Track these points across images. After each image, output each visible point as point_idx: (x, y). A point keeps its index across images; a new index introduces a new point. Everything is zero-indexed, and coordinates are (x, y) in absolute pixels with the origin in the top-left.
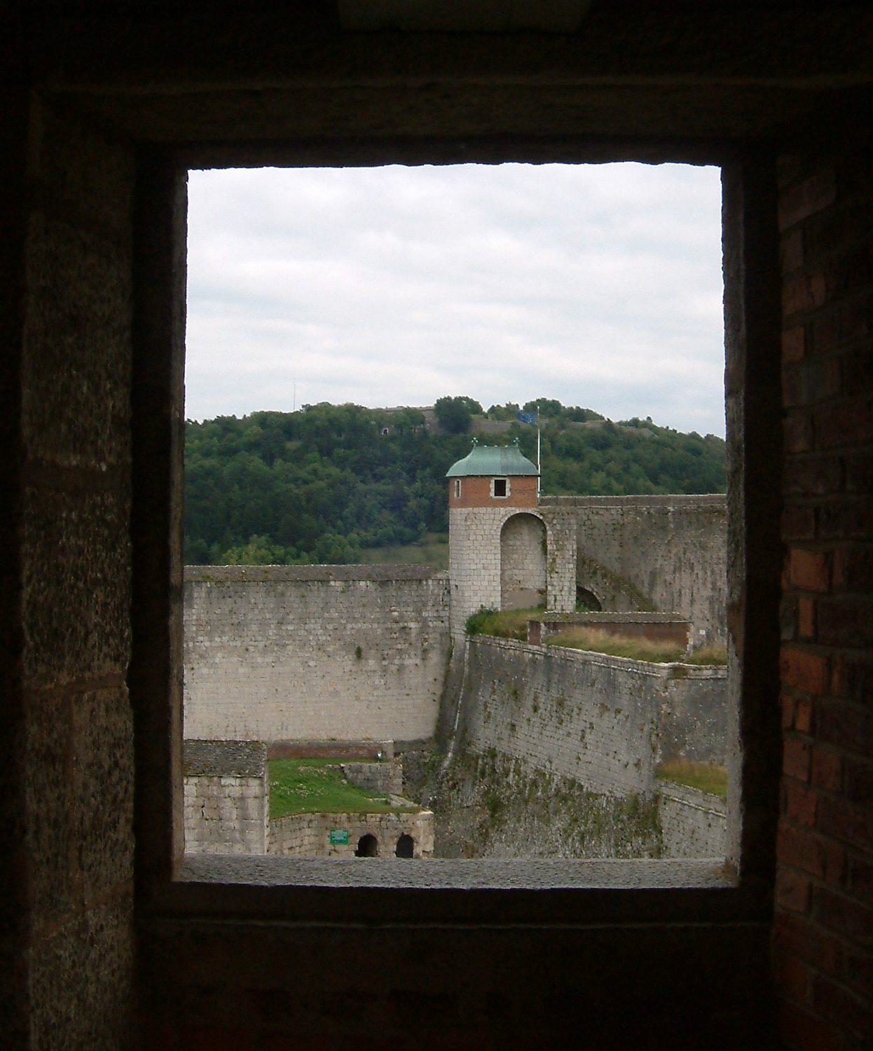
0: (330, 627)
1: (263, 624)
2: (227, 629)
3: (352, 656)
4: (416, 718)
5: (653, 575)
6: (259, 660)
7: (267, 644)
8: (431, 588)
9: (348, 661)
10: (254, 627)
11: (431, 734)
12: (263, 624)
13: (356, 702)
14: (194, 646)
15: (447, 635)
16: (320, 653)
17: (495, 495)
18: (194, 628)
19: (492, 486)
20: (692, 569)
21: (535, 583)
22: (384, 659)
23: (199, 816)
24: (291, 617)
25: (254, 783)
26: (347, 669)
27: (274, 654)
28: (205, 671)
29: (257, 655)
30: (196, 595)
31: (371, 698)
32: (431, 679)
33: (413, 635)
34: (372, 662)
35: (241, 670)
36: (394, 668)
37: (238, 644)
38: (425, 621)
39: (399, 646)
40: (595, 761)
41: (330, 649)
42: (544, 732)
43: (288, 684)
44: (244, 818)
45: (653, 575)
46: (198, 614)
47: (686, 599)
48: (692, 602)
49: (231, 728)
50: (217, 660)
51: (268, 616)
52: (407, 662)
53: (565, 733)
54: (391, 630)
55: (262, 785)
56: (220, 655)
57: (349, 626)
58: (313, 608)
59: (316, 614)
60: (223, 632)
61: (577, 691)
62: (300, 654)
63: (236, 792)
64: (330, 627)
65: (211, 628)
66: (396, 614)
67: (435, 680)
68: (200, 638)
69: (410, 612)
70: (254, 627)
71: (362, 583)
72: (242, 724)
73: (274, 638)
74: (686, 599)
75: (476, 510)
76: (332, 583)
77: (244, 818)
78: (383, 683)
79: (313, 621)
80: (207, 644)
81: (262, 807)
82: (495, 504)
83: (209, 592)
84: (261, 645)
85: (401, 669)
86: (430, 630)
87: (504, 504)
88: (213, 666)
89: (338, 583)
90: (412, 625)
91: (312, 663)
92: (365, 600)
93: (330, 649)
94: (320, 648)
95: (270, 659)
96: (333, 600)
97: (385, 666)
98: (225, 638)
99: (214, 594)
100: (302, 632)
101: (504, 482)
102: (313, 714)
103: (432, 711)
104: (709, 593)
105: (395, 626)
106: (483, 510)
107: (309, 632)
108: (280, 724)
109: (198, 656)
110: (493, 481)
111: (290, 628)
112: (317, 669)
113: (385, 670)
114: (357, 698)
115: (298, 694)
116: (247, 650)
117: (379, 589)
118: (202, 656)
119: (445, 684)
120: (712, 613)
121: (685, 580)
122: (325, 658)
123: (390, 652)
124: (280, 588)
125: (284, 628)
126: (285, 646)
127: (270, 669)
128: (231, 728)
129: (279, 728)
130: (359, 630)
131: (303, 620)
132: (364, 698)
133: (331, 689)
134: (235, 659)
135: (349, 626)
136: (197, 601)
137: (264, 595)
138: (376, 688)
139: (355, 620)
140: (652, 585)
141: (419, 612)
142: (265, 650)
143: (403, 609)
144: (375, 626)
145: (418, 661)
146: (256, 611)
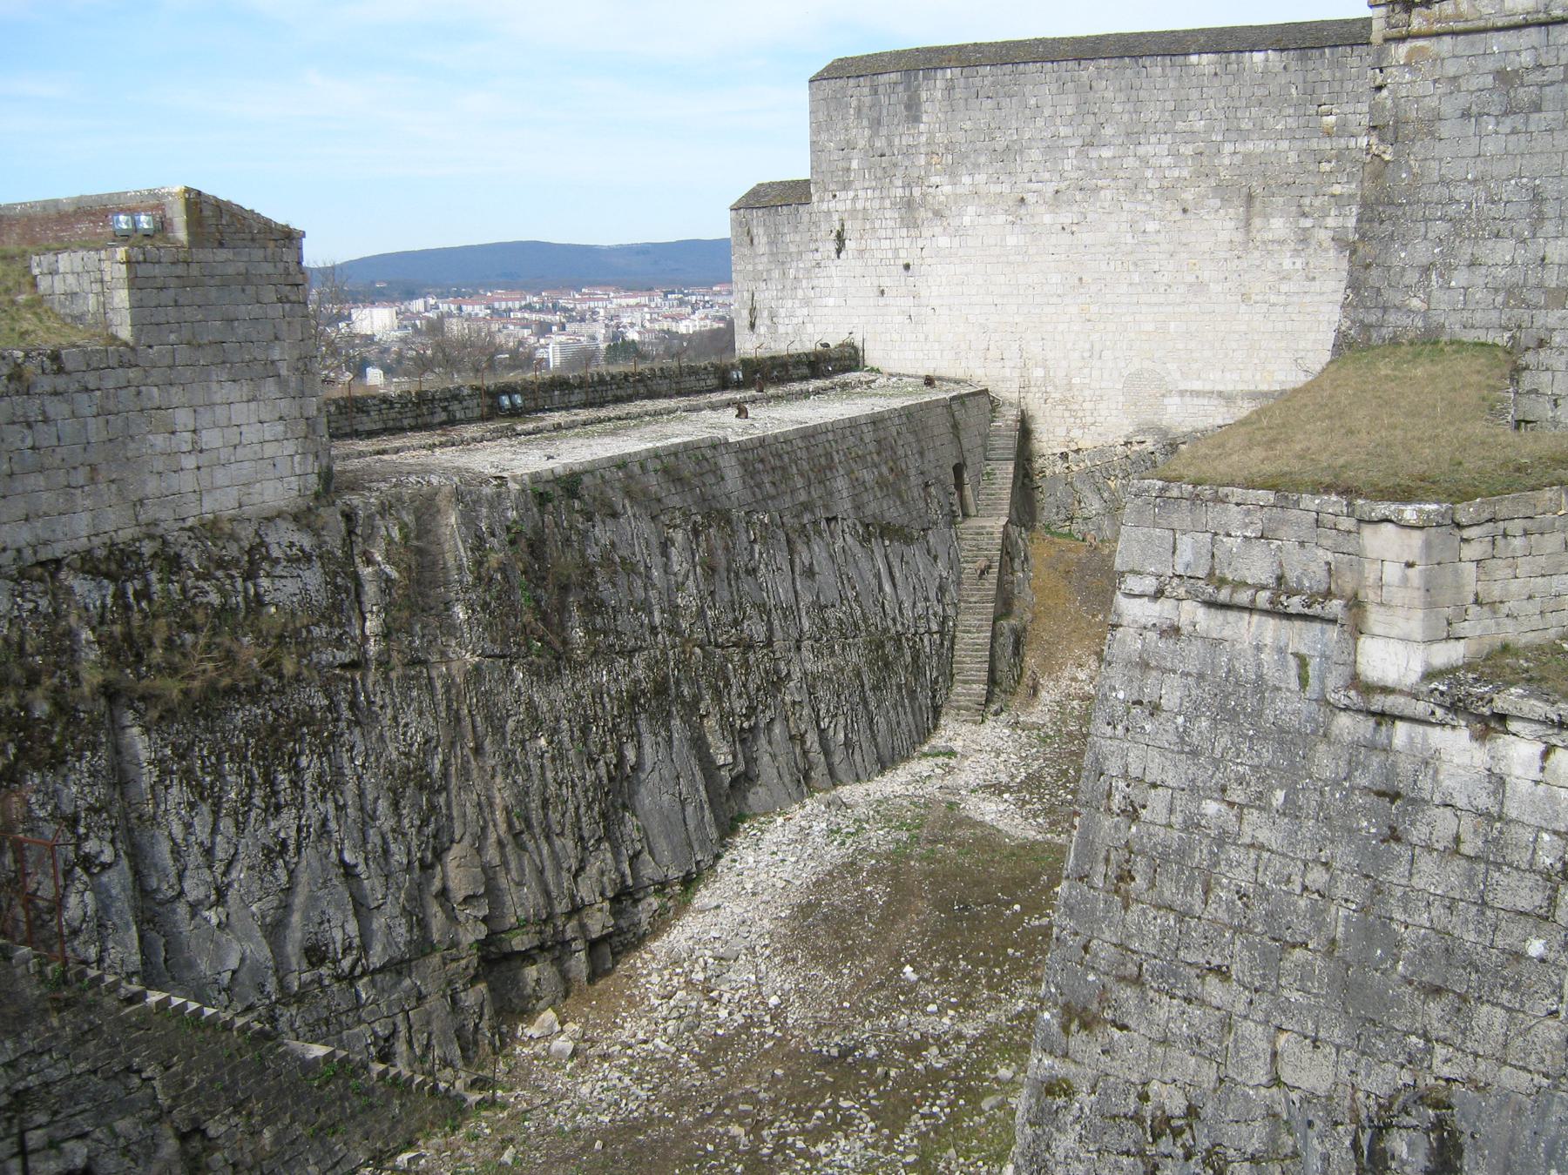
0: (1188, 150)
1: (1053, 148)
2: (982, 159)
6: (1047, 219)
7: (1063, 186)
9: (1222, 224)
10: (1035, 154)
12: (1053, 148)
13: (1243, 307)
14: (924, 195)
16: (1168, 206)
18: (922, 160)
22: (1305, 215)
24: (1108, 131)
26: (1224, 236)
27: (1075, 208)
28: (943, 241)
29: (1042, 209)
30: (924, 95)
31: (1273, 299)
35: (1011, 240)
37: (1006, 188)
39: (1337, 189)
41: (1188, 196)
43: (1104, 267)
46: (931, 134)
49: (994, 353)
50: (967, 220)
51: (1063, 131)
56: (971, 210)
57: (1228, 148)
58: (1151, 114)
59: (1160, 125)
60: (977, 166)
64: (1188, 150)
65: (957, 160)
66: (1331, 119)
68: (935, 180)
70: (1035, 154)
71: (1258, 57)
76: (1194, 59)
78: (1298, 266)
79: (1153, 139)
80: (947, 189)
83: (950, 88)
84: (1050, 189)
88: (960, 232)
89: (1205, 58)
92: (1260, 92)
93: (1188, 196)
94: (1168, 191)
95: (1066, 217)
96: (1195, 94)
97: (1305, 230)
98: (981, 178)
99: (958, 94)
100: (1130, 162)
102: (1150, 327)
105: (1326, 145)
107: (1144, 161)
108: (1088, 346)
109: (930, 215)
111: (1106, 153)
112: (1160, 238)
113: (1304, 238)
114: (1245, 297)
116: (1022, 200)
117: (1293, 66)
118: (938, 214)
122: (1178, 215)
123: (1317, 203)
125: (1093, 153)
126: (1097, 189)
127: (1065, 238)
128: (994, 353)
129: (1087, 354)
131: (1133, 136)
132: (1259, 298)
133: (1191, 279)
134: (1001, 219)
135: (1228, 148)
136: (927, 107)
137: (1054, 88)
139: (1244, 135)
143: (1348, 108)
144: (1284, 145)
146: (1040, 122)
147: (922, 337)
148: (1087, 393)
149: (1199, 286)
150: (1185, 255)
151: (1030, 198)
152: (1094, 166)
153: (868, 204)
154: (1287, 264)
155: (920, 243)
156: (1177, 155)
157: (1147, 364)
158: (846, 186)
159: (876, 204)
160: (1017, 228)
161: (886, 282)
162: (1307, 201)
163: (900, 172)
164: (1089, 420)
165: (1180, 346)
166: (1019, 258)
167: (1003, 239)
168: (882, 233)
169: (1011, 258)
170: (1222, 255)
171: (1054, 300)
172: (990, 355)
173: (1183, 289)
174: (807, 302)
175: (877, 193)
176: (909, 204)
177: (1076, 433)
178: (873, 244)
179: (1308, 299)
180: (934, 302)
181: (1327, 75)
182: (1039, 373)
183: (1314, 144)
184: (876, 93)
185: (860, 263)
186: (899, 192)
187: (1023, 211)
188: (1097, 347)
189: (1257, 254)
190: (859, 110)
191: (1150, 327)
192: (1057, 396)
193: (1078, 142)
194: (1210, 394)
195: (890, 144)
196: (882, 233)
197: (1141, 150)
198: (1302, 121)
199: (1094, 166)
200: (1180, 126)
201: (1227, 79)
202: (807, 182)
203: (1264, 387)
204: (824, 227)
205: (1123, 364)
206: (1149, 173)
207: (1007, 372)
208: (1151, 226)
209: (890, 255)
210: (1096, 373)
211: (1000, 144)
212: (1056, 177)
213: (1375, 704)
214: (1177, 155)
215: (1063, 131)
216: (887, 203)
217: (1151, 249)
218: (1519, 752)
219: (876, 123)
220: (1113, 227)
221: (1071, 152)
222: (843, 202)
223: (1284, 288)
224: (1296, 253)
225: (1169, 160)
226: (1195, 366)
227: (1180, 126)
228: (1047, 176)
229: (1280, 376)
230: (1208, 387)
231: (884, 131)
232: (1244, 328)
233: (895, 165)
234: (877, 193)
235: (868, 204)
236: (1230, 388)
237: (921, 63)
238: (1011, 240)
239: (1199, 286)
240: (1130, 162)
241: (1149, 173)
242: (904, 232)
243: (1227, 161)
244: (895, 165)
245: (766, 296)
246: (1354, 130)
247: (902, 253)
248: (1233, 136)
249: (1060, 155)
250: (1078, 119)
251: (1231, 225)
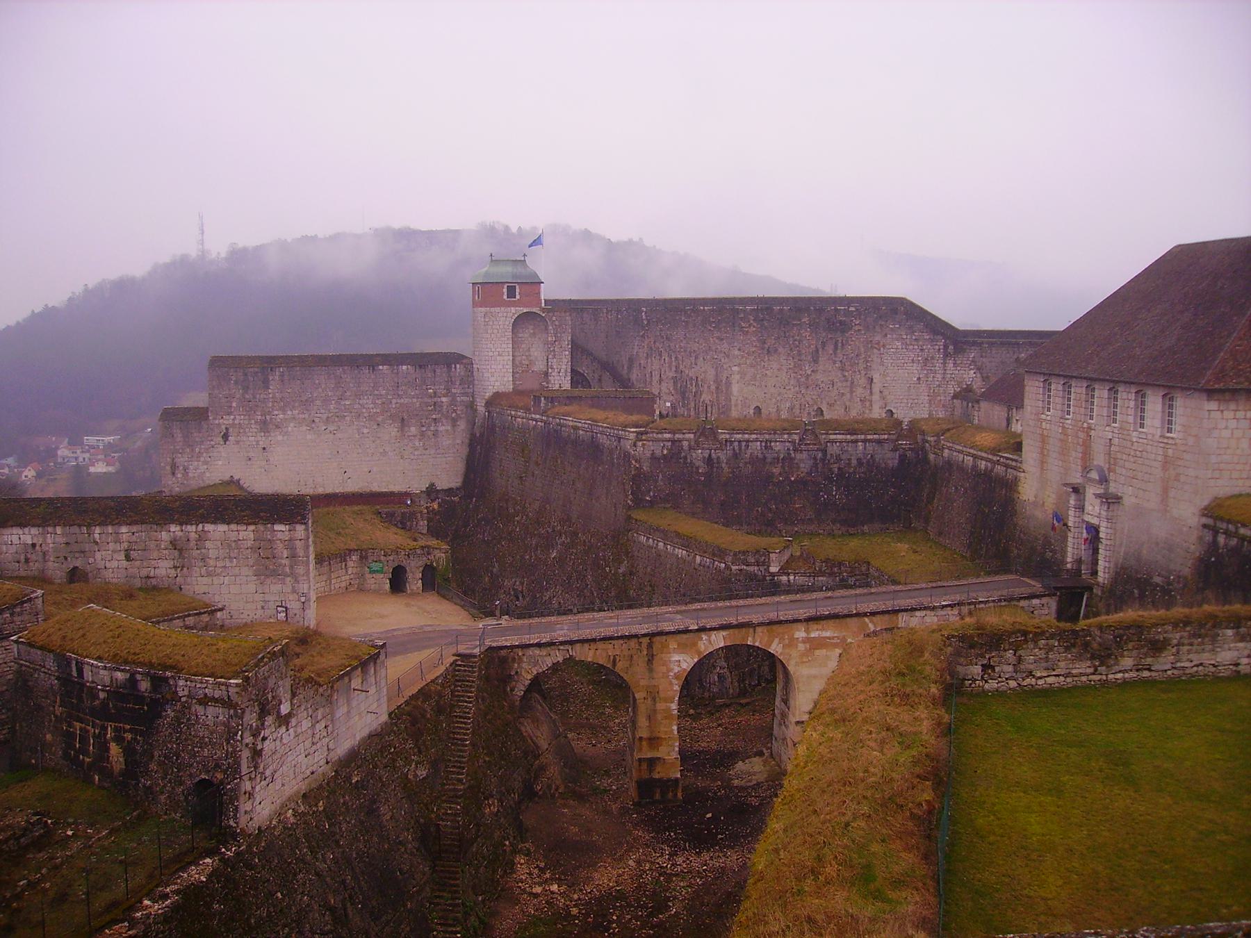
0: (379, 402)
1: (326, 401)
3: (398, 424)
5: (631, 361)
9: (392, 430)
11: (459, 485)
15: (471, 406)
19: (505, 290)
20: (661, 355)
21: (539, 366)
23: (256, 555)
25: (300, 528)
28: (280, 438)
34: (413, 429)
35: (309, 437)
36: (430, 433)
38: (454, 396)
41: (380, 419)
44: (293, 556)
45: (631, 361)
47: (656, 378)
48: (661, 381)
49: (302, 483)
52: (441, 428)
54: (427, 405)
55: (306, 530)
63: (286, 536)
64: (379, 402)
69: (441, 389)
70: (318, 403)
74: (656, 378)
75: (493, 309)
77: (293, 556)
81: (307, 547)
82: (509, 305)
83: (282, 375)
84: (325, 416)
85: (436, 434)
87: (514, 304)
90: (444, 399)
93: (380, 419)
94: (371, 418)
95: (331, 428)
100: (357, 406)
103: (460, 467)
104: (672, 374)
106: (498, 309)
113: (423, 434)
118: (278, 427)
119: (470, 445)
120: (675, 389)
121: (655, 364)
124: (339, 371)
128: (302, 483)
135: (394, 401)
140: (630, 368)
141: (449, 390)
149: (385, 453)
151: (317, 420)
158: (229, 414)
161: (251, 454)
174: (206, 463)
176: (264, 422)
183: (426, 400)
190: (236, 382)
204: (217, 431)
208: (365, 431)
211: (304, 399)
213: (773, 575)
218: (792, 577)
219: (246, 389)
222: (228, 420)
237: (269, 363)
238: (309, 437)
245: (181, 460)
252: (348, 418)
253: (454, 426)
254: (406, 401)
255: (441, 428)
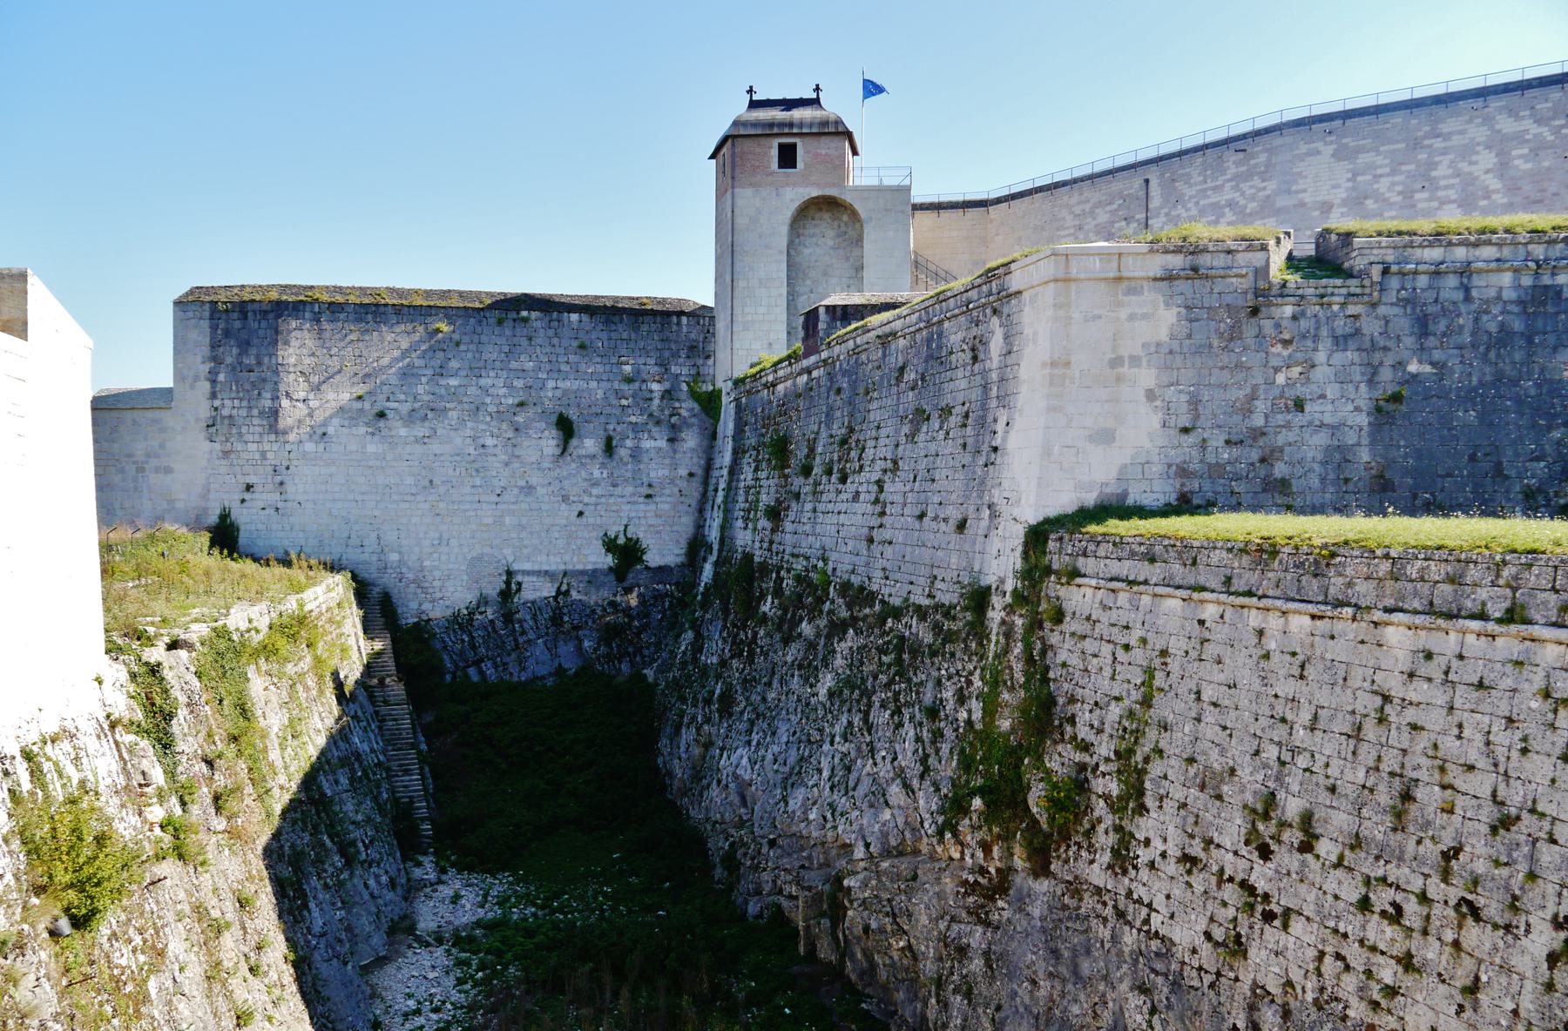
4: (658, 532)
6: (403, 432)
8: (685, 329)
16: (504, 426)
17: (780, 167)
19: (775, 152)
24: (454, 364)
27: (427, 424)
29: (399, 423)
31: (586, 499)
32: (683, 472)
33: (656, 402)
35: (371, 448)
39: (633, 419)
40: (900, 537)
41: (520, 419)
42: (820, 507)
43: (450, 471)
49: (354, 541)
51: (418, 362)
52: (647, 444)
53: (850, 496)
54: (619, 395)
59: (498, 364)
61: (874, 405)
62: (469, 424)
64: (519, 383)
67: (691, 475)
71: (574, 317)
72: (374, 535)
73: (426, 398)
79: (492, 374)
84: (405, 408)
85: (636, 454)
86: (683, 396)
90: (655, 387)
91: (490, 442)
95: (420, 430)
100: (472, 390)
101: (794, 146)
102: (489, 520)
105: (625, 387)
107: (485, 391)
110: (775, 145)
111: (453, 382)
112: (498, 451)
114: (565, 499)
115: (468, 490)
125: (443, 382)
127: (419, 449)
130: (566, 392)
131: (476, 371)
133: (523, 483)
134: (362, 430)
135: (551, 384)
138: (596, 484)
142: (411, 418)
143: (641, 361)
144: (593, 384)
145: (662, 443)
147: (287, 527)
148: (437, 574)
149: (529, 489)
150: (516, 465)
151: (391, 415)
152: (443, 391)
153: (235, 412)
154: (597, 474)
155: (288, 447)
156: (511, 387)
157: (487, 550)
159: (243, 412)
160: (376, 438)
162: (611, 427)
163: (269, 386)
164: (438, 595)
165: (514, 535)
166: (378, 463)
167: (364, 446)
168: (250, 438)
169: (371, 463)
170: (546, 465)
171: (408, 498)
172: (351, 542)
173: (516, 491)
175: (245, 403)
177: (426, 606)
178: (239, 446)
179: (612, 500)
180: (300, 498)
181: (625, 335)
182: (394, 557)
184: (246, 318)
185: (224, 462)
186: (268, 403)
187: (382, 424)
188: (445, 536)
189: (574, 465)
191: (489, 520)
192: (411, 576)
193: (429, 372)
194: (538, 573)
195: (259, 363)
196: (250, 438)
197: (482, 382)
198: (608, 368)
199: (443, 391)
200: (514, 365)
201: (551, 333)
202: (169, 391)
203: (580, 567)
205: (466, 550)
206: (488, 400)
207: (366, 557)
209: (257, 456)
210: (444, 557)
212: (410, 399)
214: (511, 387)
215: (418, 362)
216: (255, 412)
217: (491, 459)
220: (458, 441)
221: (424, 380)
223: (595, 491)
224: (603, 465)
225: (504, 390)
226: (525, 551)
227: (514, 365)
228: (402, 397)
229: (593, 559)
230: (536, 568)
231: (253, 351)
232: (564, 522)
233: (264, 380)
234: (245, 403)
235: (235, 412)
236: (553, 567)
238: (371, 448)
239: (529, 489)
240: (472, 390)
241: (488, 400)
242: (273, 437)
243: (550, 394)
244: (264, 380)
246: (645, 377)
247: (269, 455)
248: (555, 375)
249: (414, 380)
250: (430, 354)
251: (554, 442)
252: (453, 415)
253: (671, 440)
254: (576, 385)
255: (647, 444)
